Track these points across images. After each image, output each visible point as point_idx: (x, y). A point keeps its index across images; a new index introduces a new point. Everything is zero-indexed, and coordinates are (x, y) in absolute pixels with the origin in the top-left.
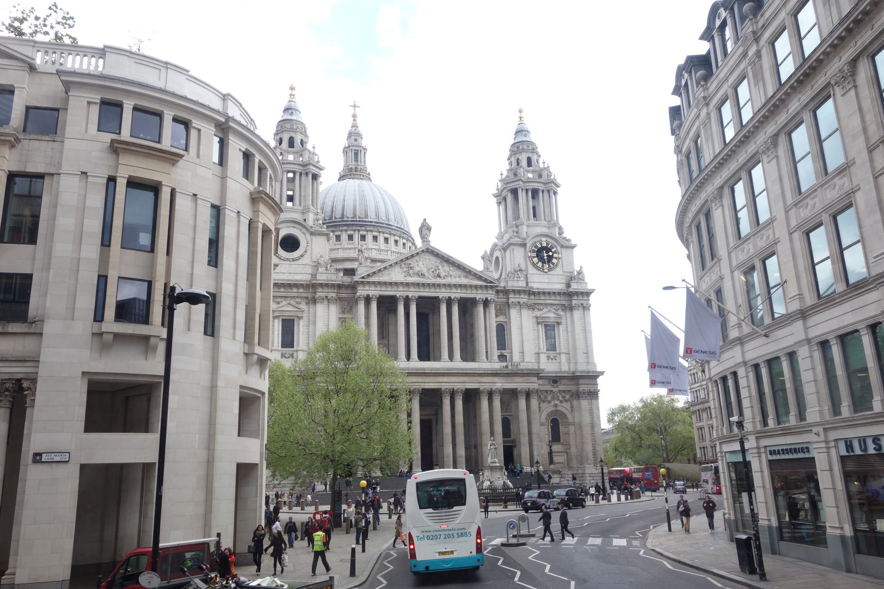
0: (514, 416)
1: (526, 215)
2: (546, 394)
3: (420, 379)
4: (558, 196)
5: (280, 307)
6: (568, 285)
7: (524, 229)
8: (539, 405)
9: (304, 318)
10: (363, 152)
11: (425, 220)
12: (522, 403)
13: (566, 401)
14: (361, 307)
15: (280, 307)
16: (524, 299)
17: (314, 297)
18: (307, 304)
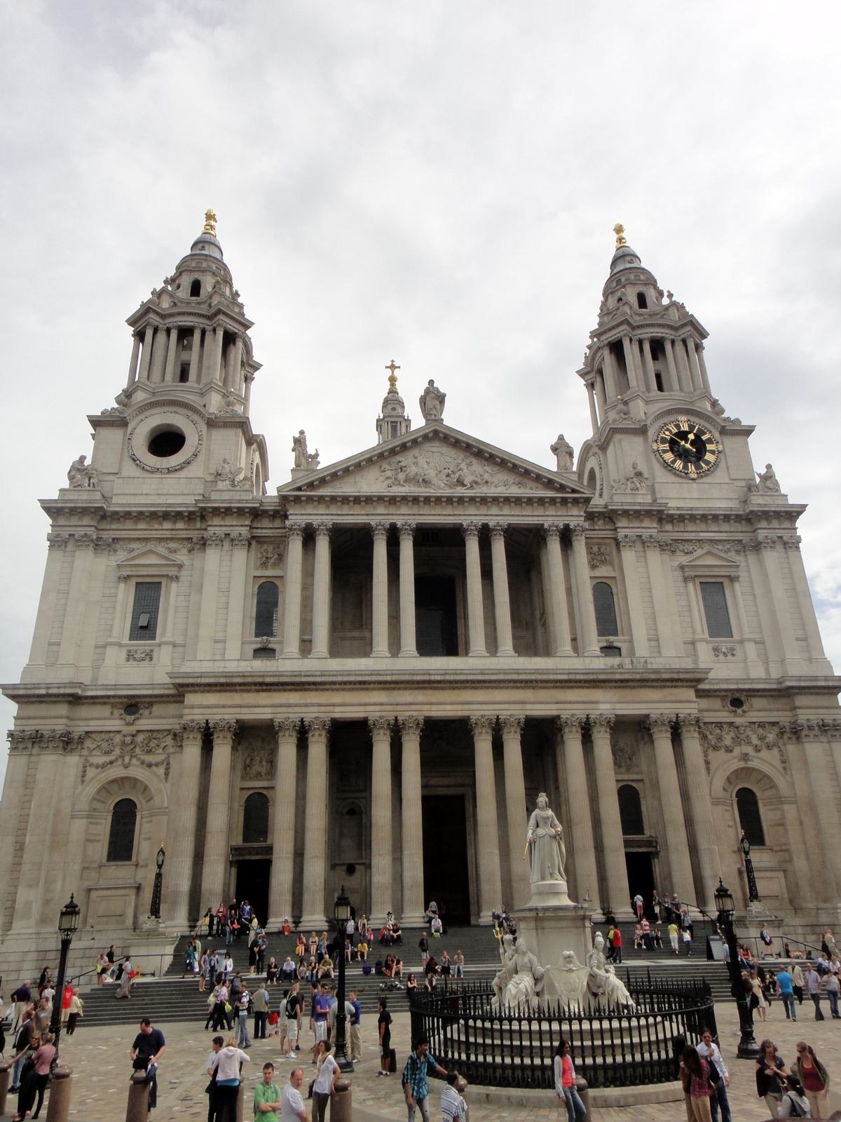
0: (647, 782)
1: (642, 384)
2: (718, 731)
3: (420, 696)
4: (706, 354)
5: (133, 558)
6: (745, 501)
7: (639, 410)
8: (706, 756)
9: (181, 579)
10: (404, 425)
11: (431, 382)
12: (663, 744)
13: (769, 747)
14: (295, 548)
15: (133, 558)
16: (650, 528)
17: (203, 538)
18: (190, 551)
